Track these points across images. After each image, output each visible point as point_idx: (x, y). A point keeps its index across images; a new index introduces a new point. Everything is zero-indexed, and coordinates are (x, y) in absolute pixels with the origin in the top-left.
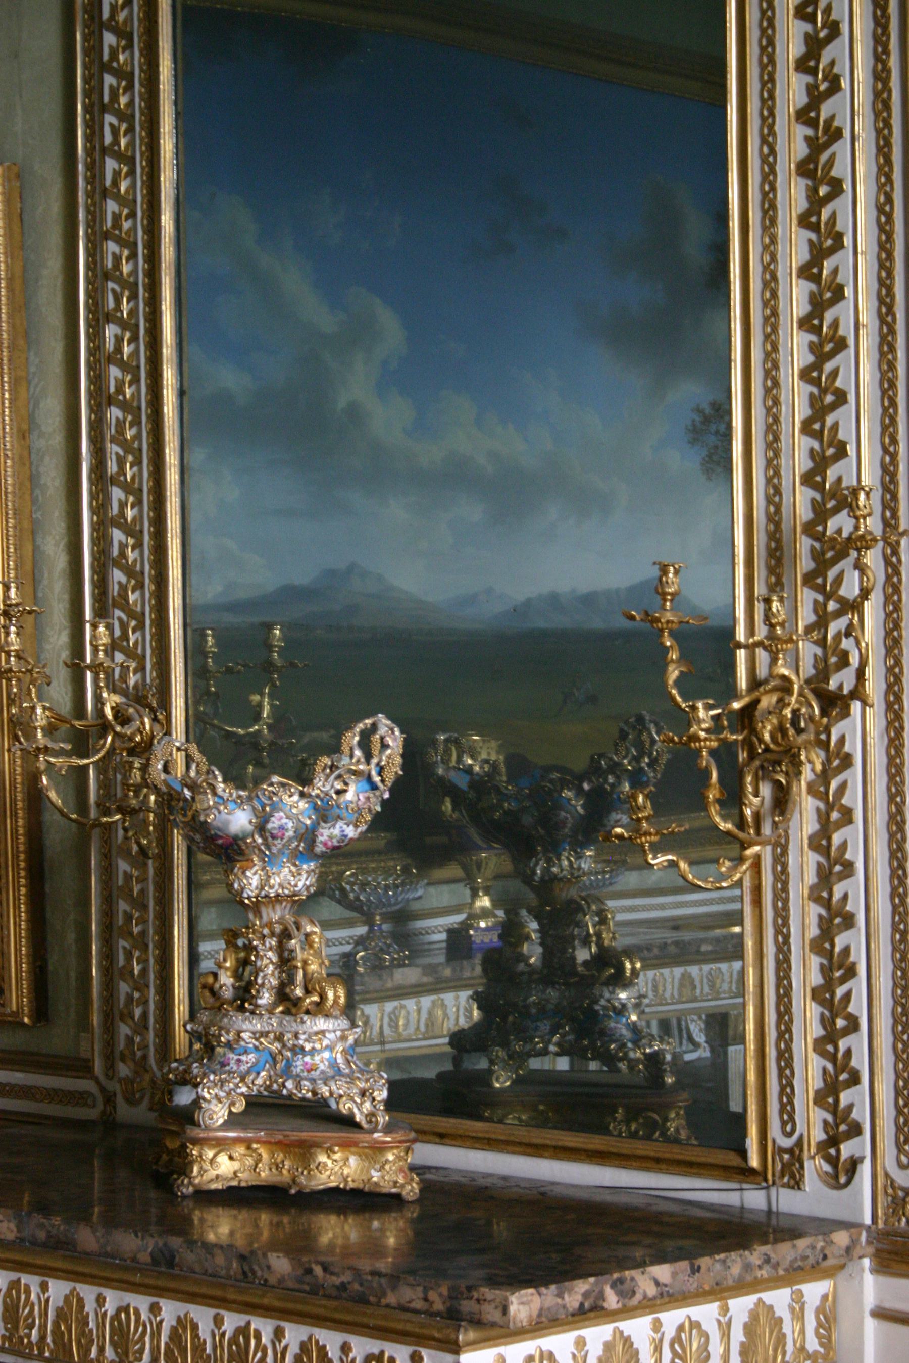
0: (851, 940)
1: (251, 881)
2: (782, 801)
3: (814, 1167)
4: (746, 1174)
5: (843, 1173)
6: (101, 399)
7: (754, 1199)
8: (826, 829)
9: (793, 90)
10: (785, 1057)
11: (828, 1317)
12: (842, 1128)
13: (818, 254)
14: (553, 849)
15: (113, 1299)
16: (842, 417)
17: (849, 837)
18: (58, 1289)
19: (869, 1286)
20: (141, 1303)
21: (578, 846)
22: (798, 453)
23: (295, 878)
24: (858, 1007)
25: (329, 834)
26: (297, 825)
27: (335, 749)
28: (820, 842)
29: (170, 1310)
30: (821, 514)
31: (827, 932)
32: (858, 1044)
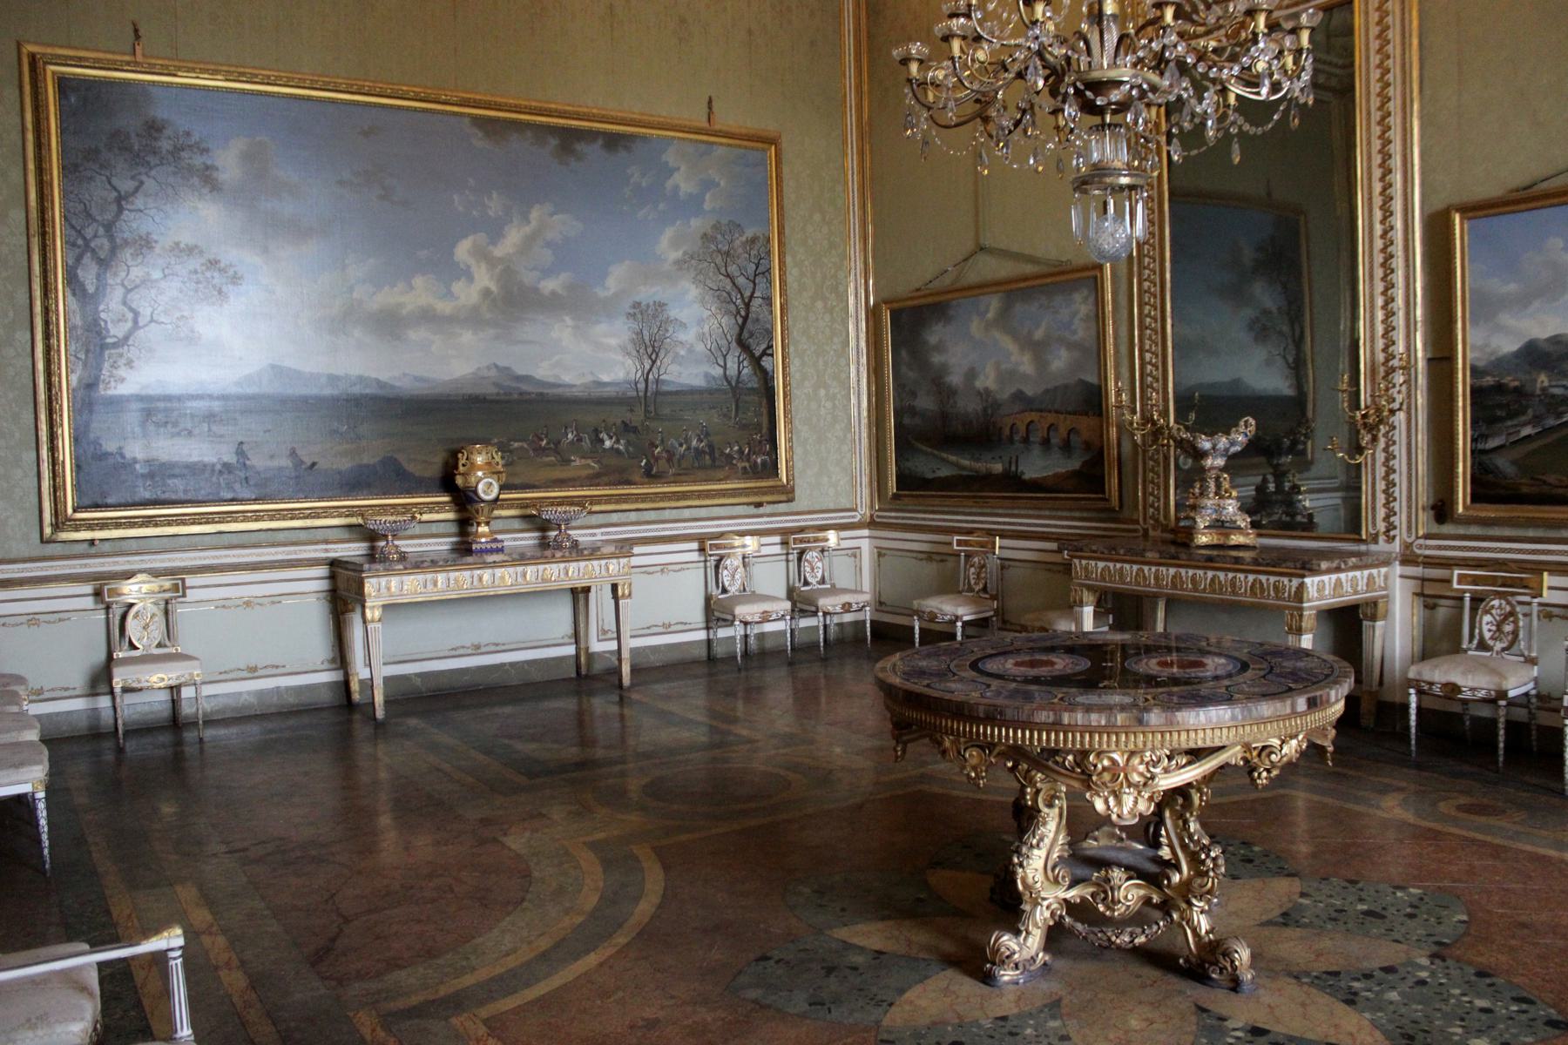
0: (1395, 477)
1: (1209, 462)
2: (1375, 439)
3: (1382, 538)
4: (1361, 541)
5: (1391, 539)
6: (1142, 327)
7: (1363, 548)
8: (1388, 446)
9: (1379, 244)
10: (1374, 509)
11: (1386, 577)
12: (1391, 527)
13: (1386, 289)
14: (1280, 455)
15: (1191, 572)
16: (1394, 333)
17: (1395, 449)
18: (1172, 571)
19: (1398, 569)
20: (1200, 572)
21: (1287, 454)
22: (1380, 344)
23: (1220, 462)
24: (1397, 494)
25: (1233, 450)
26: (1217, 449)
27: (1237, 425)
28: (1386, 450)
29: (1210, 574)
30: (1387, 360)
31: (1387, 474)
32: (1396, 505)
